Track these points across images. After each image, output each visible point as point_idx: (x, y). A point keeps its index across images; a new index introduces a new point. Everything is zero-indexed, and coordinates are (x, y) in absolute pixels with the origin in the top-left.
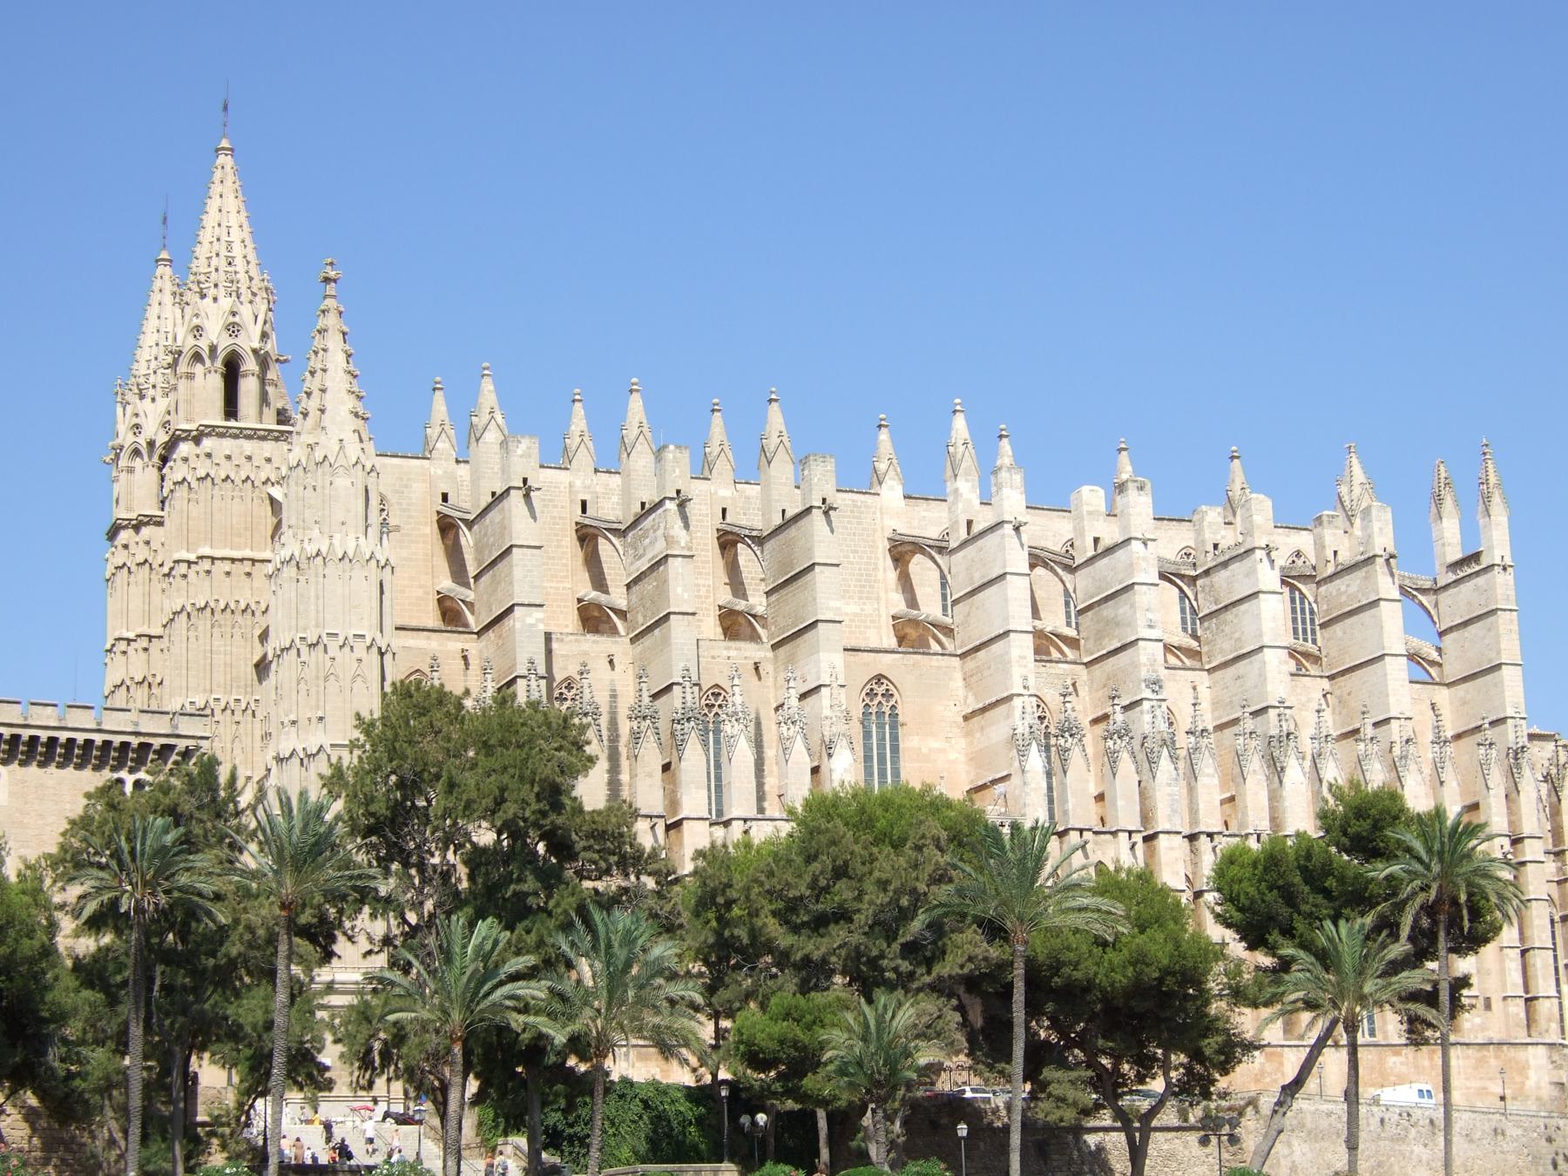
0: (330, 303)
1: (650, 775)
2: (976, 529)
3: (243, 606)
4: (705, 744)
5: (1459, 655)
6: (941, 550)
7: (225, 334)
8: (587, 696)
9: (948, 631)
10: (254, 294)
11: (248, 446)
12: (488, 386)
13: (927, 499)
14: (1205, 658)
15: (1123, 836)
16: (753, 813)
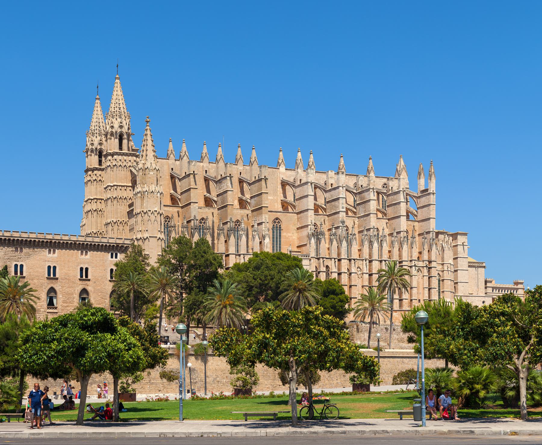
0: (148, 128)
1: (222, 243)
2: (302, 182)
3: (124, 197)
4: (235, 237)
5: (421, 214)
6: (293, 186)
7: (119, 128)
8: (208, 225)
9: (294, 207)
10: (126, 117)
11: (125, 158)
12: (184, 145)
13: (291, 170)
14: (357, 214)
15: (333, 260)
16: (246, 253)
